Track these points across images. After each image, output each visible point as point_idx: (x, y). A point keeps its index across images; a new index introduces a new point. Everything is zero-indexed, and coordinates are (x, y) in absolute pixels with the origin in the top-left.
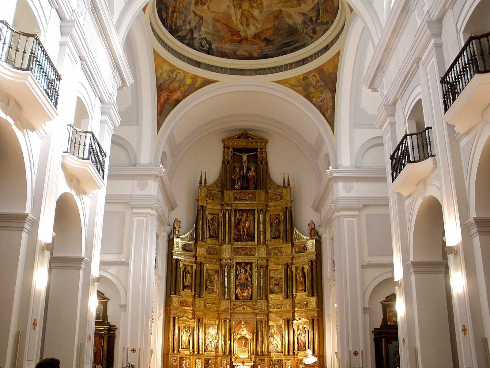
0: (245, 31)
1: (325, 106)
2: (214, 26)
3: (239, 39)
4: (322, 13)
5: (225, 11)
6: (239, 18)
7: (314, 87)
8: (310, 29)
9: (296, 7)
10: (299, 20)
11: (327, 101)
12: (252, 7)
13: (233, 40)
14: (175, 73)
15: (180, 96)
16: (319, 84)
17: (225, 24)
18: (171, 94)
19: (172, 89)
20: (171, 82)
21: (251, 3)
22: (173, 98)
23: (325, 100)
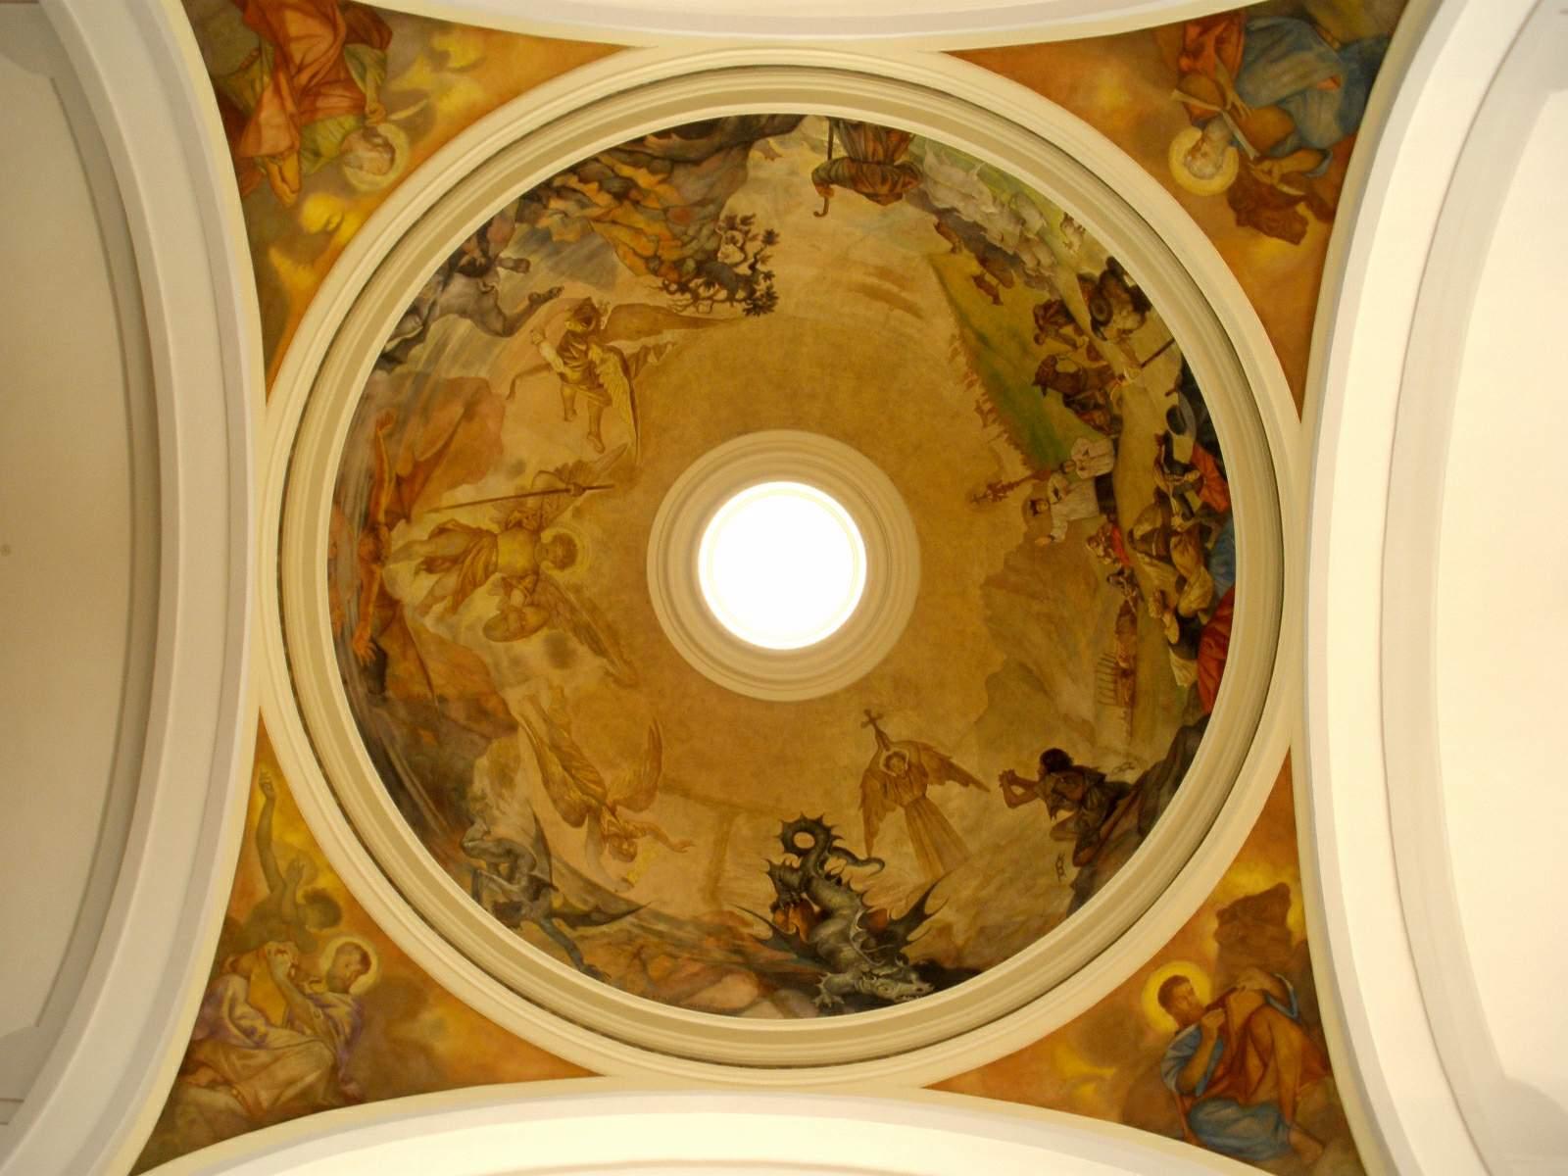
0: (407, 550)
1: (238, 1064)
2: (455, 386)
3: (381, 517)
4: (604, 934)
5: (501, 451)
6: (465, 518)
7: (300, 974)
8: (504, 892)
9: (555, 801)
10: (508, 822)
11: (265, 1067)
12: (507, 586)
13: (382, 481)
14: (399, 140)
15: (259, 143)
16: (331, 997)
17: (447, 445)
18: (292, 89)
19: (321, 103)
20: (359, 107)
21: (522, 578)
22: (268, 95)
23: (262, 1057)
